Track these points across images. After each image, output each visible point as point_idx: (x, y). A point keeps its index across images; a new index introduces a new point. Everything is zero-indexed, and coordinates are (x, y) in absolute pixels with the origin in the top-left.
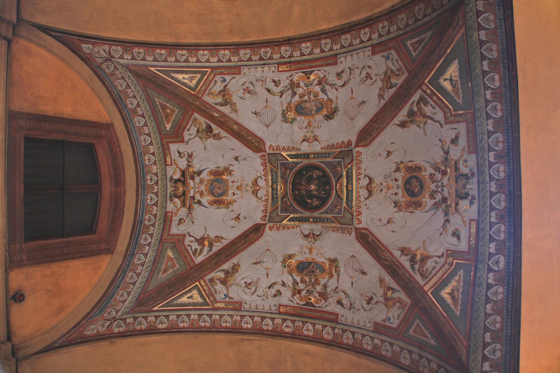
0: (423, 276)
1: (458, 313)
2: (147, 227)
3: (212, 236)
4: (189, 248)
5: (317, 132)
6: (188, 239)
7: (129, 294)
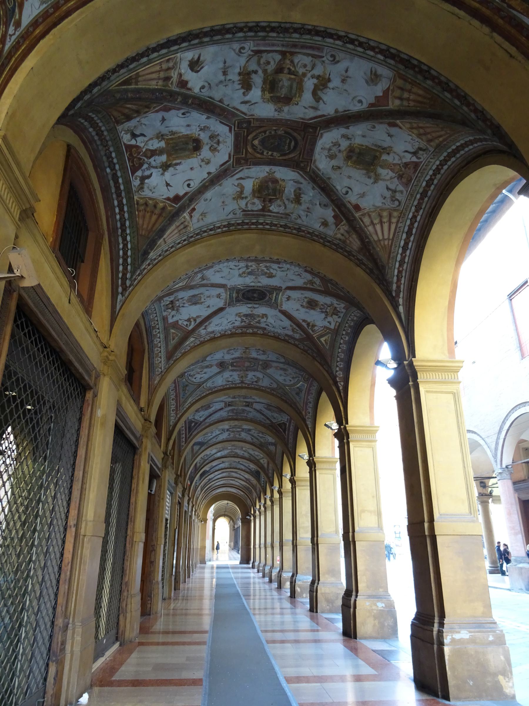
0: (313, 331)
1: (327, 348)
2: (155, 326)
3: (195, 316)
4: (183, 325)
5: (260, 280)
6: (180, 322)
7: (161, 357)
